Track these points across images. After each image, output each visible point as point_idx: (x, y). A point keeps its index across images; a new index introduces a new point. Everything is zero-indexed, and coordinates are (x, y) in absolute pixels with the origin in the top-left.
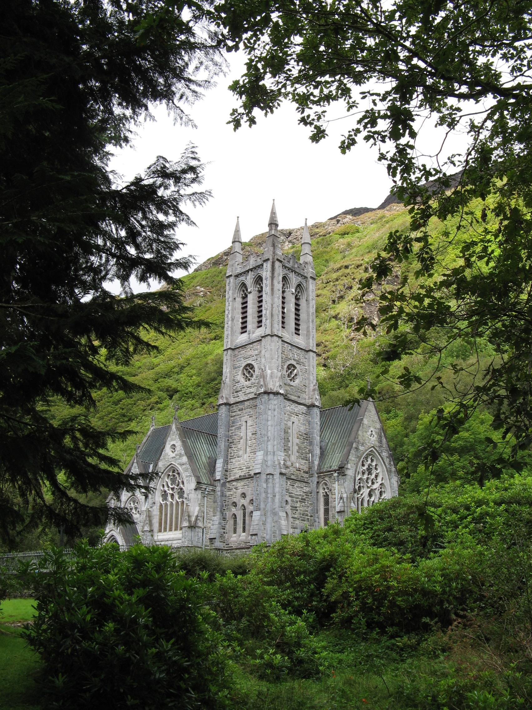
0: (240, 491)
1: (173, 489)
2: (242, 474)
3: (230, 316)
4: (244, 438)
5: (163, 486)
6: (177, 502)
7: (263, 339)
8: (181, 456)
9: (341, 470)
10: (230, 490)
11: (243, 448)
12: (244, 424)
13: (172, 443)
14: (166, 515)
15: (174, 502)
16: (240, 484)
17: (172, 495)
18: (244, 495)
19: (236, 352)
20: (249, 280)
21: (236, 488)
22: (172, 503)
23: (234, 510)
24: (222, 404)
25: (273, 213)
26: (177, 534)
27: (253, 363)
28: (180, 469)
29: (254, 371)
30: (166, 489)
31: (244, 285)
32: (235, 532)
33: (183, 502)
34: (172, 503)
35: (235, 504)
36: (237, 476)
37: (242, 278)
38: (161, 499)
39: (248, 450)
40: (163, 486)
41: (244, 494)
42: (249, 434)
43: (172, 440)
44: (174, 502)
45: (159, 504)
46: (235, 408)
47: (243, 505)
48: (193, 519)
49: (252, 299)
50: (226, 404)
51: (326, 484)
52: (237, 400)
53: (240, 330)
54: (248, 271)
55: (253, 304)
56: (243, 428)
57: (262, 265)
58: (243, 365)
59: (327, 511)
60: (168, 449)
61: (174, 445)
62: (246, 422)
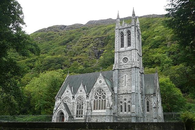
0: (124, 98)
1: (100, 95)
2: (124, 92)
3: (118, 42)
4: (125, 81)
5: (96, 94)
7: (132, 50)
9: (154, 94)
10: (119, 97)
14: (97, 104)
15: (101, 100)
16: (124, 96)
17: (100, 98)
18: (125, 99)
19: (120, 53)
20: (125, 31)
21: (122, 97)
23: (121, 104)
24: (116, 69)
25: (134, 12)
27: (127, 57)
28: (104, 89)
30: (97, 95)
32: (121, 111)
33: (105, 100)
35: (121, 102)
37: (122, 30)
38: (94, 99)
39: (126, 85)
40: (96, 94)
41: (125, 99)
42: (127, 80)
44: (101, 100)
45: (94, 100)
46: (120, 71)
47: (125, 103)
48: (111, 106)
49: (125, 38)
50: (118, 69)
51: (148, 98)
52: (121, 68)
53: (121, 47)
54: (124, 28)
55: (126, 39)
56: (124, 77)
57: (131, 27)
59: (148, 107)
60: (98, 82)
61: (101, 81)
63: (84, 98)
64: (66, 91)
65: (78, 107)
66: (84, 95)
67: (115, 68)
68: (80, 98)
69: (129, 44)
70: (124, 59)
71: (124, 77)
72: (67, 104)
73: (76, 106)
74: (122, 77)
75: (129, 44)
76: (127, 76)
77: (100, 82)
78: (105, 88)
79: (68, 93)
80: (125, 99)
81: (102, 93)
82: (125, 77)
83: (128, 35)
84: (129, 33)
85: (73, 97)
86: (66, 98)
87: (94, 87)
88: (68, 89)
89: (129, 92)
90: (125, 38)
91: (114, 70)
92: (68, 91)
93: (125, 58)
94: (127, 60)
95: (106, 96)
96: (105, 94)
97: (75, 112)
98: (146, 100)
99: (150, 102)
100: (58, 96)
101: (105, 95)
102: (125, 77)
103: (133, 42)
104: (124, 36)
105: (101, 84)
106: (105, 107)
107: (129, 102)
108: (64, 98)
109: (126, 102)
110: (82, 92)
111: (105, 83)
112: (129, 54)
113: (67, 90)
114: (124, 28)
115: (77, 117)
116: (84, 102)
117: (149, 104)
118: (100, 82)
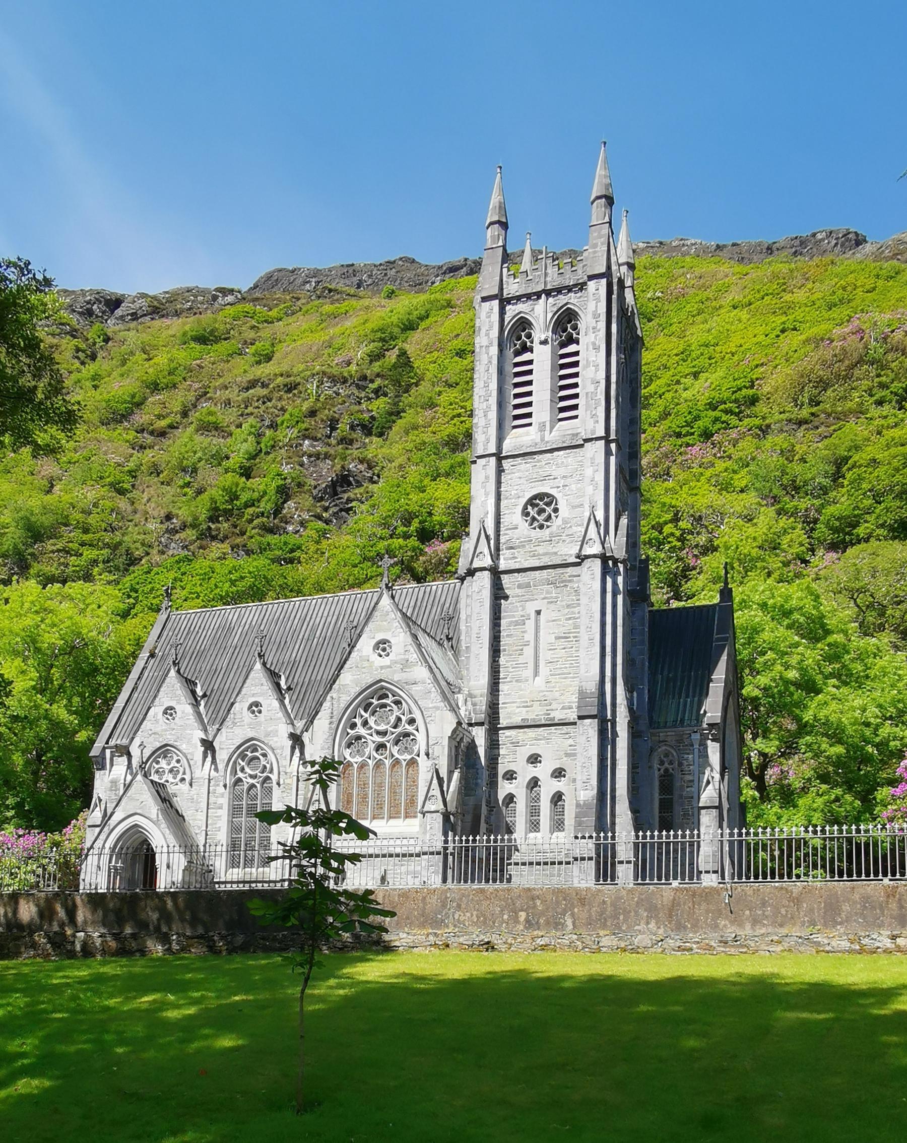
1: (383, 733)
4: (532, 644)
6: (397, 762)
8: (406, 665)
11: (531, 665)
12: (533, 615)
13: (380, 636)
15: (388, 762)
18: (534, 759)
20: (541, 314)
22: (379, 764)
26: (412, 826)
27: (553, 492)
29: (556, 510)
31: (523, 324)
33: (412, 763)
34: (379, 764)
36: (517, 720)
39: (543, 670)
42: (546, 637)
43: (380, 630)
49: (542, 357)
54: (538, 295)
58: (528, 495)
62: (538, 613)
63: (278, 751)
64: (156, 711)
65: (235, 811)
66: (275, 733)
67: (476, 564)
68: (249, 751)
69: (565, 404)
70: (531, 502)
71: (530, 625)
72: (171, 789)
73: (223, 798)
74: (517, 623)
75: (565, 404)
76: (554, 615)
77: (382, 646)
78: (415, 688)
79: (166, 718)
80: (534, 759)
81: (393, 719)
82: (537, 622)
83: (563, 345)
84: (565, 324)
85: (208, 746)
86: (164, 751)
87: (346, 677)
88: (172, 692)
89: (558, 716)
90: (542, 357)
91: (471, 573)
92: (169, 711)
93: (540, 496)
94: (549, 510)
95: (421, 737)
96: (412, 721)
97: (222, 836)
98: (656, 766)
99: (678, 775)
100: (112, 743)
101: (410, 729)
102: (537, 622)
103: (591, 388)
104: (536, 346)
105: (386, 661)
106: (412, 801)
107: (559, 773)
108: (147, 753)
109: (543, 771)
110: (261, 717)
111: (414, 656)
112: (561, 471)
113: (164, 699)
114: (538, 295)
115: (233, 863)
116: (274, 777)
117: (677, 784)
118: (382, 646)
